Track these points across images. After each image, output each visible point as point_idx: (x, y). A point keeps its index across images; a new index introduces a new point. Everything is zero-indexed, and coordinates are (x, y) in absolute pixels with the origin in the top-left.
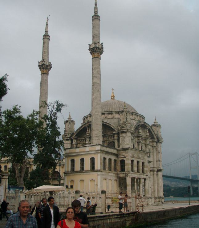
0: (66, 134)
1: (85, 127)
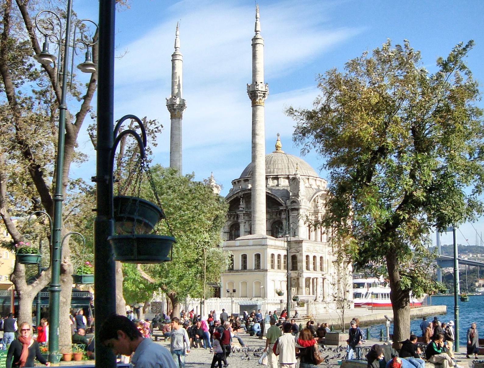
1: (237, 197)
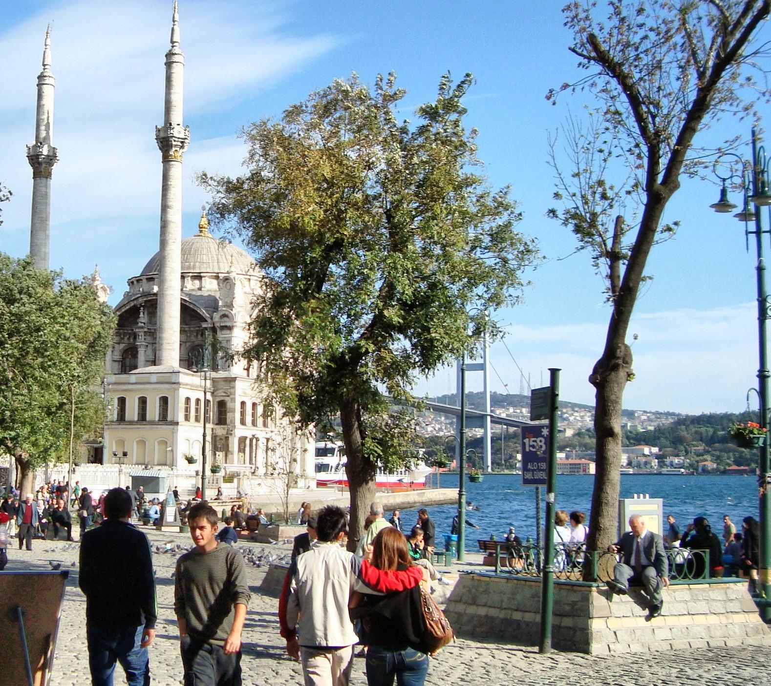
1: (135, 306)
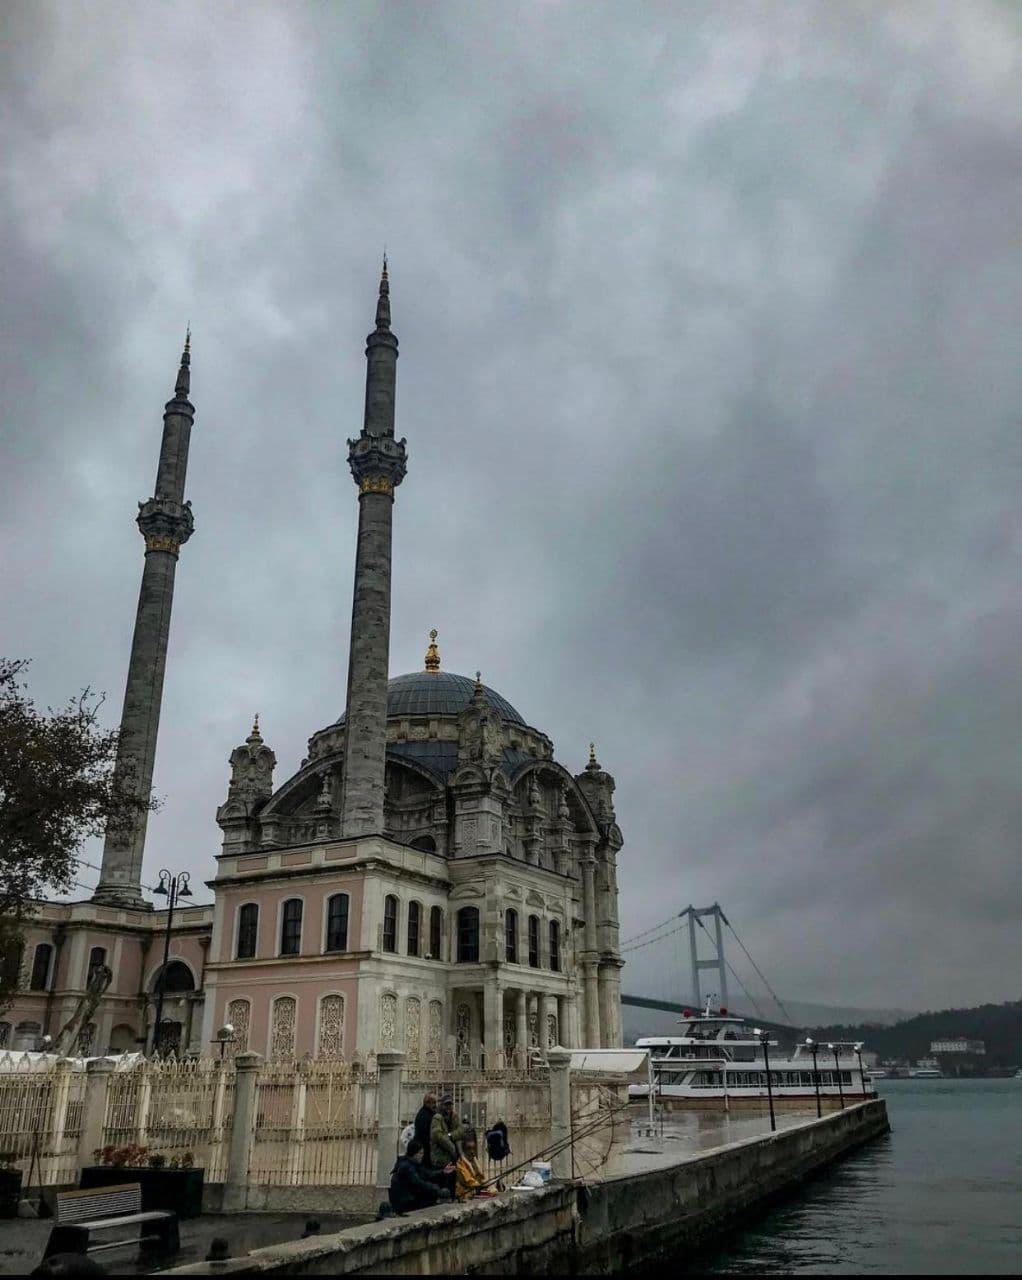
0: (233, 804)
1: (315, 775)
